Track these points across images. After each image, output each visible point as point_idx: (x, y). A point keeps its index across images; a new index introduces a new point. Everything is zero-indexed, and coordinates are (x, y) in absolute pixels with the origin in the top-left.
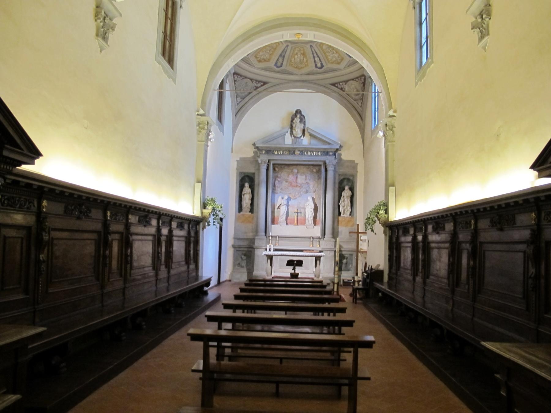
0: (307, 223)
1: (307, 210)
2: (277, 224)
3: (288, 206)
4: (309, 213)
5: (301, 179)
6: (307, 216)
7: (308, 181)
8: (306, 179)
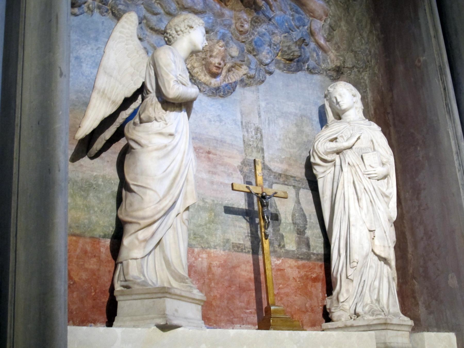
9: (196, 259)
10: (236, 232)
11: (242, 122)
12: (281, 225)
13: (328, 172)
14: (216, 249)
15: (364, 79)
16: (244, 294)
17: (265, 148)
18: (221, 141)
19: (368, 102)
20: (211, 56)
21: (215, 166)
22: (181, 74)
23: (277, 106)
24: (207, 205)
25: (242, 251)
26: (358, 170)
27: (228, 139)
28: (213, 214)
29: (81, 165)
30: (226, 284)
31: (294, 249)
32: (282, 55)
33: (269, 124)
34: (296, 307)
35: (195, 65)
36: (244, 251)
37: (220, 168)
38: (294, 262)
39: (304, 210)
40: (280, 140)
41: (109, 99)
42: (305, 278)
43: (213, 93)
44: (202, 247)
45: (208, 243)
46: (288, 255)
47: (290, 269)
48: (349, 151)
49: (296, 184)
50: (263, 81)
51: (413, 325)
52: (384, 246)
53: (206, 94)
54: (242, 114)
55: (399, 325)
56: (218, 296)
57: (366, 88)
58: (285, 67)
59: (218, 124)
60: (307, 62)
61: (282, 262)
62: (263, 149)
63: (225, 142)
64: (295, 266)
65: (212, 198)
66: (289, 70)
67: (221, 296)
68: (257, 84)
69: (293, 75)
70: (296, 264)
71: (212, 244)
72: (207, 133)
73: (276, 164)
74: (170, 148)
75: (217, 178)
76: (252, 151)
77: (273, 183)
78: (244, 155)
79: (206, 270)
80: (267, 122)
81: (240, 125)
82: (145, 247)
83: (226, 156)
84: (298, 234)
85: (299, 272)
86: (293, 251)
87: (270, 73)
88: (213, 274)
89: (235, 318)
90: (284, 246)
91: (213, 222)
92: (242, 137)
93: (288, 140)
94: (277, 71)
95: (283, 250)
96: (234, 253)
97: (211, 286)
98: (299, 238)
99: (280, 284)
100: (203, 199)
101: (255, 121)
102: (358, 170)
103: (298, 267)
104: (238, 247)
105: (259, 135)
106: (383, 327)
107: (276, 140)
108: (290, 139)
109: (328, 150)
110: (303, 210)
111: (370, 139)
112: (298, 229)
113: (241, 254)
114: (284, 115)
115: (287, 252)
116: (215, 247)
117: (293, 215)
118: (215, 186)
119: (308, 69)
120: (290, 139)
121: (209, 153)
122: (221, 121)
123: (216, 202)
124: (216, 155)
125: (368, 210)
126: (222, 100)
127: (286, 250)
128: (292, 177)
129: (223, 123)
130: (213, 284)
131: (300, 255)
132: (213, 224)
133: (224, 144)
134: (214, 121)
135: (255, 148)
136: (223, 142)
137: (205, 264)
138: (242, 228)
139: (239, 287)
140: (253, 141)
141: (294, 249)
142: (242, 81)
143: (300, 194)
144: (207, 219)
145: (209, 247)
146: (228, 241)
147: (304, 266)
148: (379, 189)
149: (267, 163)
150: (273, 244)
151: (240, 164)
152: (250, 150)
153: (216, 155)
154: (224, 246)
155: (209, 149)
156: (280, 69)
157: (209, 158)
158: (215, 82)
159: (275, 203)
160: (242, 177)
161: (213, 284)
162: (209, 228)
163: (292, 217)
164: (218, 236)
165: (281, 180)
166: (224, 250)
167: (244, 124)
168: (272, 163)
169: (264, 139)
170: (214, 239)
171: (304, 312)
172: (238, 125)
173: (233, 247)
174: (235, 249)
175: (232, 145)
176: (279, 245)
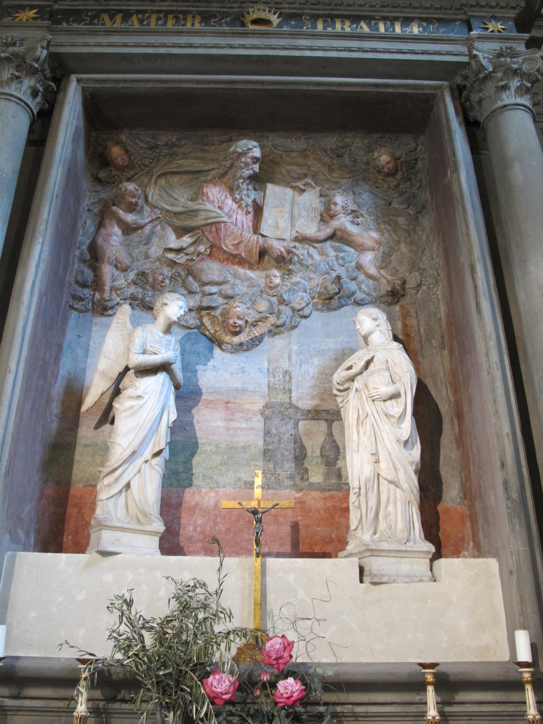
0: (361, 535)
1: (352, 407)
2: (80, 547)
3: (187, 396)
4: (379, 447)
5: (289, 213)
6: (357, 466)
7: (344, 222)
8: (327, 215)
9: (203, 498)
11: (268, 369)
12: (306, 459)
13: (346, 400)
15: (436, 294)
17: (293, 388)
18: (242, 390)
19: (440, 318)
20: (228, 318)
21: (233, 414)
23: (313, 346)
26: (363, 394)
27: (250, 387)
28: (226, 457)
29: (103, 431)
30: (234, 519)
31: (321, 480)
32: (319, 297)
33: (300, 365)
34: (318, 538)
35: (217, 329)
37: (238, 415)
38: (319, 494)
39: (337, 441)
40: (313, 377)
41: (107, 377)
42: (332, 508)
43: (236, 349)
45: (217, 483)
46: (312, 487)
47: (313, 501)
48: (359, 377)
49: (329, 417)
50: (295, 327)
51: (434, 550)
52: (390, 469)
54: (269, 361)
55: (398, 551)
56: (224, 530)
57: (439, 303)
58: (323, 307)
59: (240, 375)
60: (352, 296)
61: (303, 495)
62: (290, 391)
63: (247, 391)
64: (320, 498)
66: (329, 309)
67: (228, 530)
68: (288, 330)
69: (337, 313)
70: (322, 495)
73: (305, 402)
74: (135, 408)
75: (233, 425)
76: (278, 394)
77: (299, 420)
78: (267, 399)
79: (213, 508)
80: (299, 363)
82: (109, 491)
84: (327, 466)
85: (324, 503)
86: (319, 483)
87: (306, 317)
90: (307, 479)
91: (224, 464)
92: (267, 383)
93: (324, 376)
94: (315, 313)
95: (306, 483)
98: (328, 470)
99: (298, 516)
101: (285, 364)
102: (363, 394)
103: (324, 499)
105: (287, 377)
106: (368, 554)
107: (308, 378)
108: (326, 374)
109: (342, 380)
110: (335, 442)
111: (385, 359)
112: (327, 461)
114: (321, 353)
115: (312, 484)
116: (224, 486)
117: (322, 448)
118: (231, 432)
119: (354, 301)
120: (326, 374)
121: (228, 403)
122: (244, 372)
123: (230, 445)
124: (235, 403)
125: (371, 434)
126: (247, 354)
127: (310, 483)
128: (324, 411)
129: (247, 374)
130: (219, 519)
131: (328, 486)
135: (281, 390)
136: (244, 391)
137: (212, 502)
139: (249, 521)
140: (280, 384)
141: (321, 480)
142: (270, 331)
143: (333, 426)
146: (239, 480)
147: (332, 497)
148: (383, 410)
149: (294, 401)
150: (294, 478)
152: (275, 393)
153: (235, 403)
156: (318, 310)
157: (227, 408)
158: (236, 340)
159: (301, 439)
160: (262, 419)
161: (219, 519)
162: (221, 470)
163: (321, 450)
164: (229, 476)
165: (310, 416)
166: (234, 488)
167: (271, 370)
168: (300, 402)
169: (294, 381)
170: (225, 479)
171: (328, 543)
172: (264, 373)
173: (245, 484)
175: (255, 392)
176: (302, 479)
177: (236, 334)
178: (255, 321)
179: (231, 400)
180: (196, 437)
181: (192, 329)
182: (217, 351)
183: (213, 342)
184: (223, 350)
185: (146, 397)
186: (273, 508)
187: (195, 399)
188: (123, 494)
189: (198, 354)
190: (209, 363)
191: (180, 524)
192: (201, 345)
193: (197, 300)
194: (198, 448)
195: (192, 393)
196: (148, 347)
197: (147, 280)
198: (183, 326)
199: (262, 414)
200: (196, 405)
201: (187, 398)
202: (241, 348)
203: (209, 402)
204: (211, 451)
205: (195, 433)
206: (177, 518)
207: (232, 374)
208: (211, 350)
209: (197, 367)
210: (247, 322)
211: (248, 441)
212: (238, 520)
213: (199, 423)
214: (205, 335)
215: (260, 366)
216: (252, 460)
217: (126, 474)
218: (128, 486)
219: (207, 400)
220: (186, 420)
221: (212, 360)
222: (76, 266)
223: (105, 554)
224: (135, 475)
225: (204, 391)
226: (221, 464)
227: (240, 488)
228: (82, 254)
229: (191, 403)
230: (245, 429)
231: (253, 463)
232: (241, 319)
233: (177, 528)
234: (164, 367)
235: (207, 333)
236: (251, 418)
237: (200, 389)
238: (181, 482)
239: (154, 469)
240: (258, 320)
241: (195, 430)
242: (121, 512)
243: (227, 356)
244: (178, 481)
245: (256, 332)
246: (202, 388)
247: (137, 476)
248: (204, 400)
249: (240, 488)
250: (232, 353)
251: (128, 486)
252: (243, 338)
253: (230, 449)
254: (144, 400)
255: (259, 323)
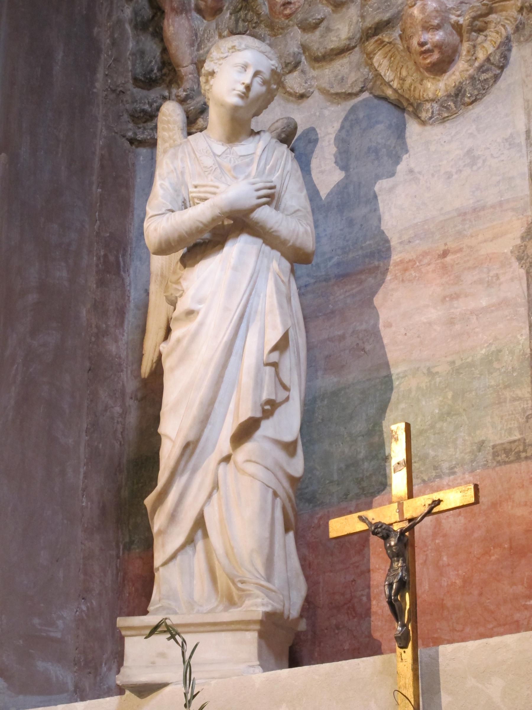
10: (502, 419)
14: (454, 473)
16: (523, 561)
18: (474, 210)
21: (458, 279)
22: (196, 183)
24: (438, 380)
25: (518, 459)
28: (450, 395)
30: (477, 550)
36: (523, 455)
44: (424, 481)
45: (436, 468)
53: (434, 122)
56: (459, 582)
63: (483, 208)
65: (449, 359)
67: (467, 581)
71: (445, 466)
72: (442, 209)
75: (461, 306)
81: (523, 143)
83: (485, 241)
88: (445, 536)
89: (500, 625)
91: (449, 414)
96: (498, 469)
97: (441, 563)
100: (429, 369)
104: (507, 452)
113: (515, 466)
121: (445, 254)
123: (458, 363)
124: (461, 250)
126: (477, 110)
129: (480, 163)
130: (445, 559)
132: (449, 419)
133: (482, 213)
134: (456, 173)
138: (520, 399)
139: (511, 548)
142: (518, 29)
144: (437, 411)
145: (439, 477)
146: (481, 445)
151: (518, 242)
153: (461, 250)
154: (472, 462)
155: (446, 244)
157: (444, 267)
161: (445, 559)
164: (460, 442)
166: (472, 471)
173: (495, 454)
174: (499, 458)
177: (440, 68)
178: (475, 19)
179: (452, 245)
180: (387, 365)
181: (357, 94)
182: (413, 128)
183: (403, 110)
184: (423, 123)
185: (202, 308)
186: (429, 513)
187: (377, 268)
188: (200, 545)
189: (376, 151)
190: (399, 168)
191: (369, 587)
192: (380, 127)
193: (355, 19)
194: (392, 389)
195: (371, 255)
196: (191, 189)
197: (259, 15)
198: (337, 94)
199: (519, 259)
200: (383, 281)
201: (361, 272)
202: (460, 99)
203: (407, 266)
204: (418, 388)
205: (385, 355)
206: (362, 573)
207: (449, 176)
208: (400, 132)
209: (377, 188)
210: (458, 28)
211: (496, 339)
212: (487, 553)
213: (389, 325)
214: (385, 99)
215: (509, 131)
216: (506, 387)
217: (189, 499)
218: (200, 523)
219: (402, 262)
220: (364, 326)
221: (405, 157)
222: (131, 45)
223: (145, 690)
224: (210, 496)
225: (394, 243)
226: (442, 417)
227: (485, 466)
228: (136, 13)
229: (371, 281)
230: (484, 310)
231: (508, 394)
232: (438, 28)
233: (364, 599)
234: (235, 224)
235: (389, 92)
236: (497, 276)
237: (387, 241)
238: (364, 484)
239: (244, 472)
240: (484, 10)
241: (383, 347)
242: (201, 585)
243: (436, 132)
244: (359, 481)
245: (487, 46)
246: (389, 234)
247: (215, 496)
248: (397, 264)
249: (485, 466)
250: (444, 120)
251: (200, 523)
252: (460, 71)
253: (457, 371)
254: (199, 318)
255: (493, 17)
